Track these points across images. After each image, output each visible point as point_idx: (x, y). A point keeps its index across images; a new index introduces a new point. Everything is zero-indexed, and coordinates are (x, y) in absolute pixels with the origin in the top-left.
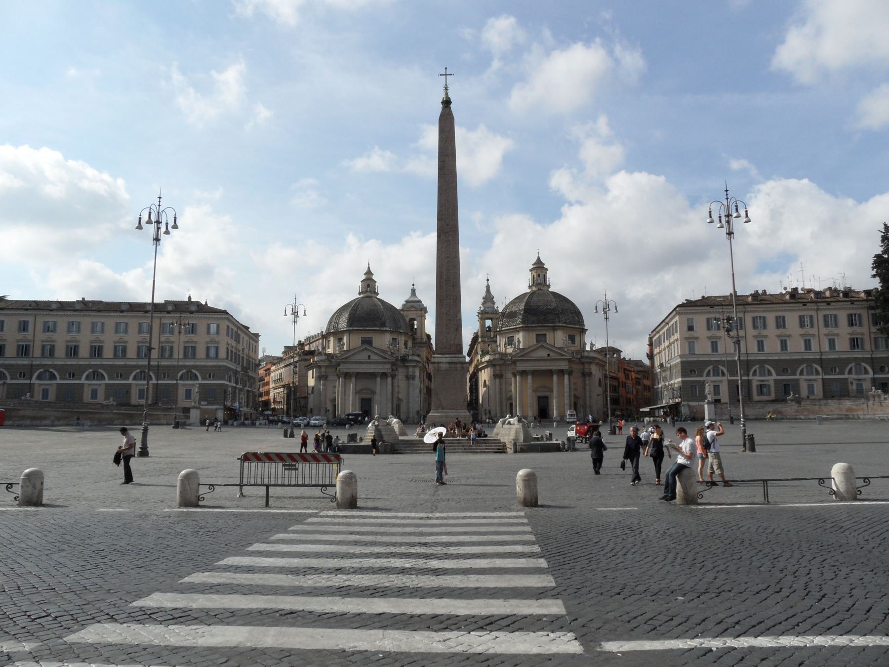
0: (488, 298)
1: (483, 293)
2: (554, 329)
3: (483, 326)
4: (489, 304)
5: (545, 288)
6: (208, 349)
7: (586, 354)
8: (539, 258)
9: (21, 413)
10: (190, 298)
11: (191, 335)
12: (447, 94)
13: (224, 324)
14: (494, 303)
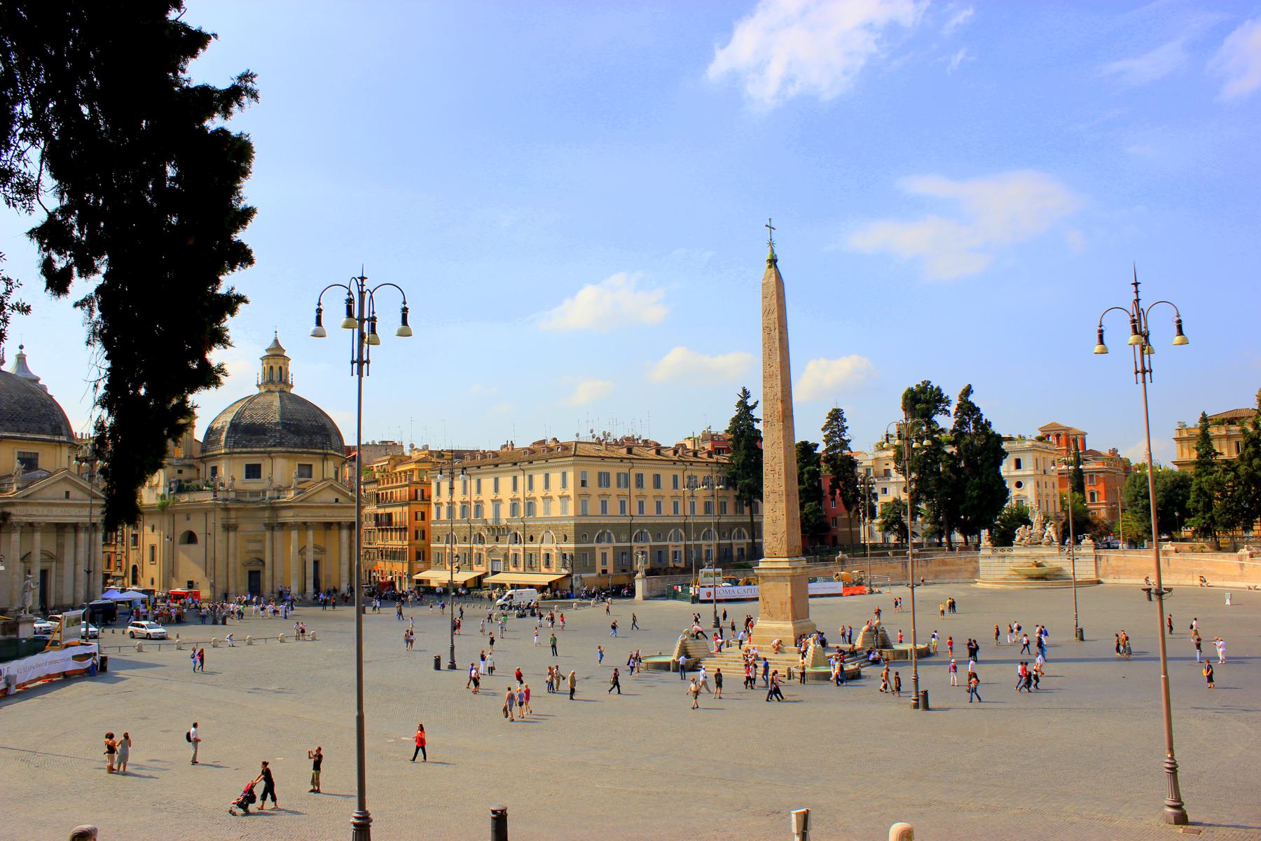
2: (325, 457)
8: (276, 341)
12: (772, 251)
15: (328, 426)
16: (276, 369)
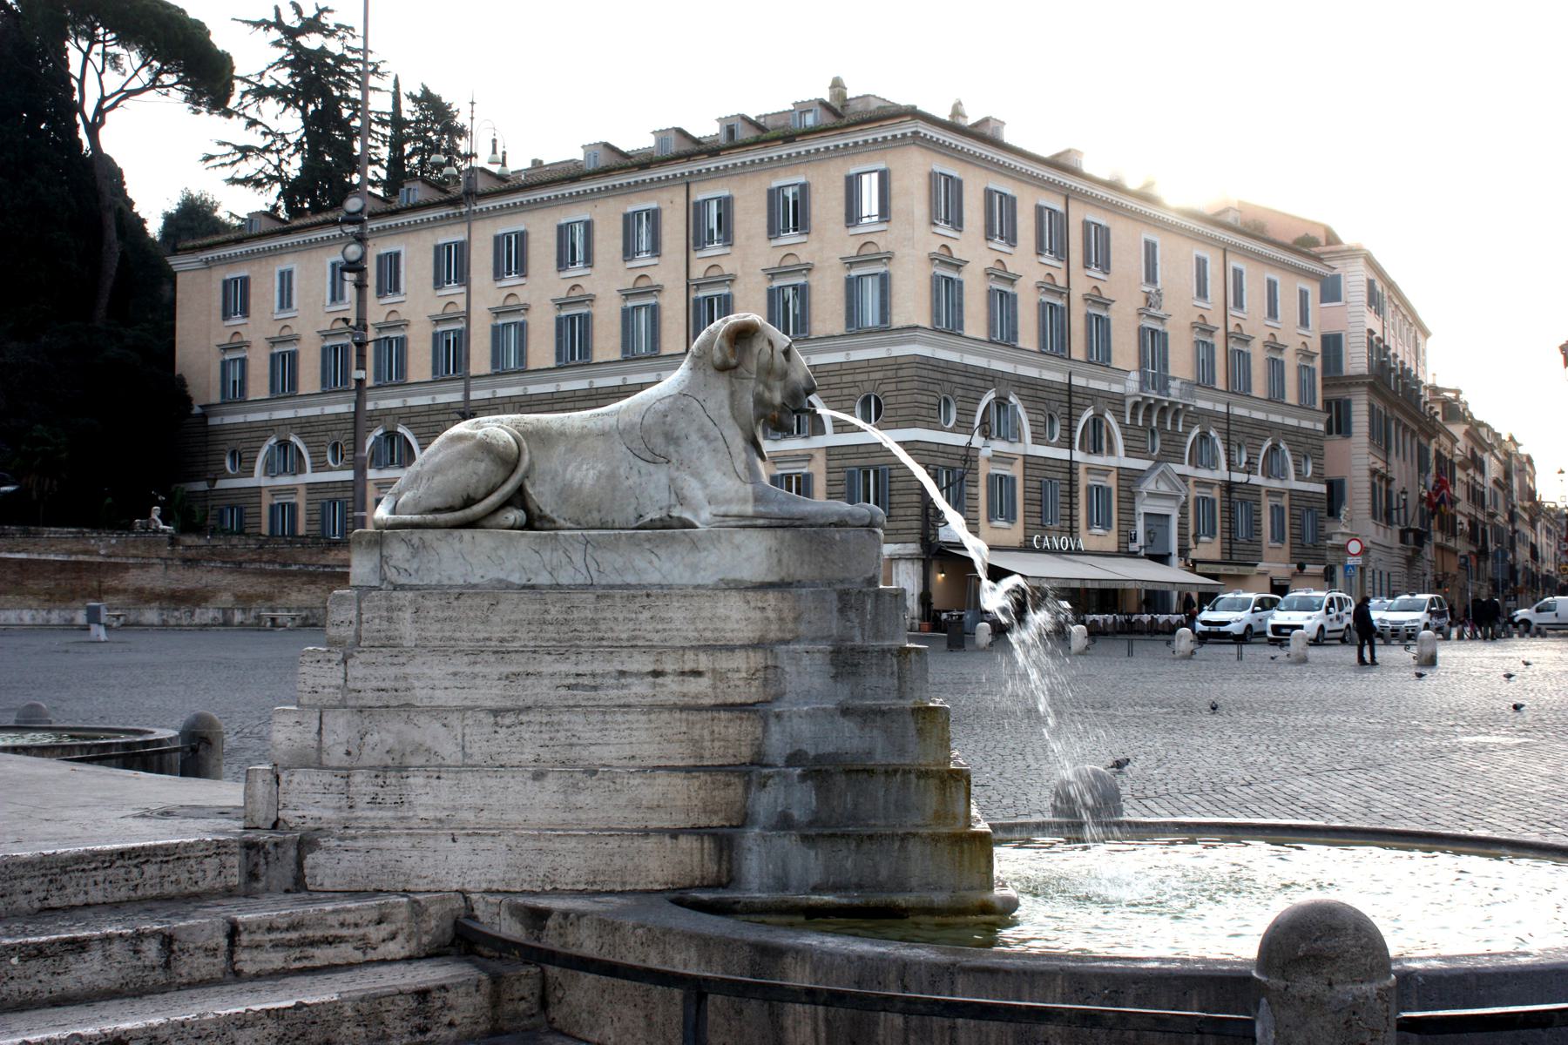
6: (852, 287)
9: (134, 579)
10: (837, 85)
11: (791, 238)
13: (913, 171)
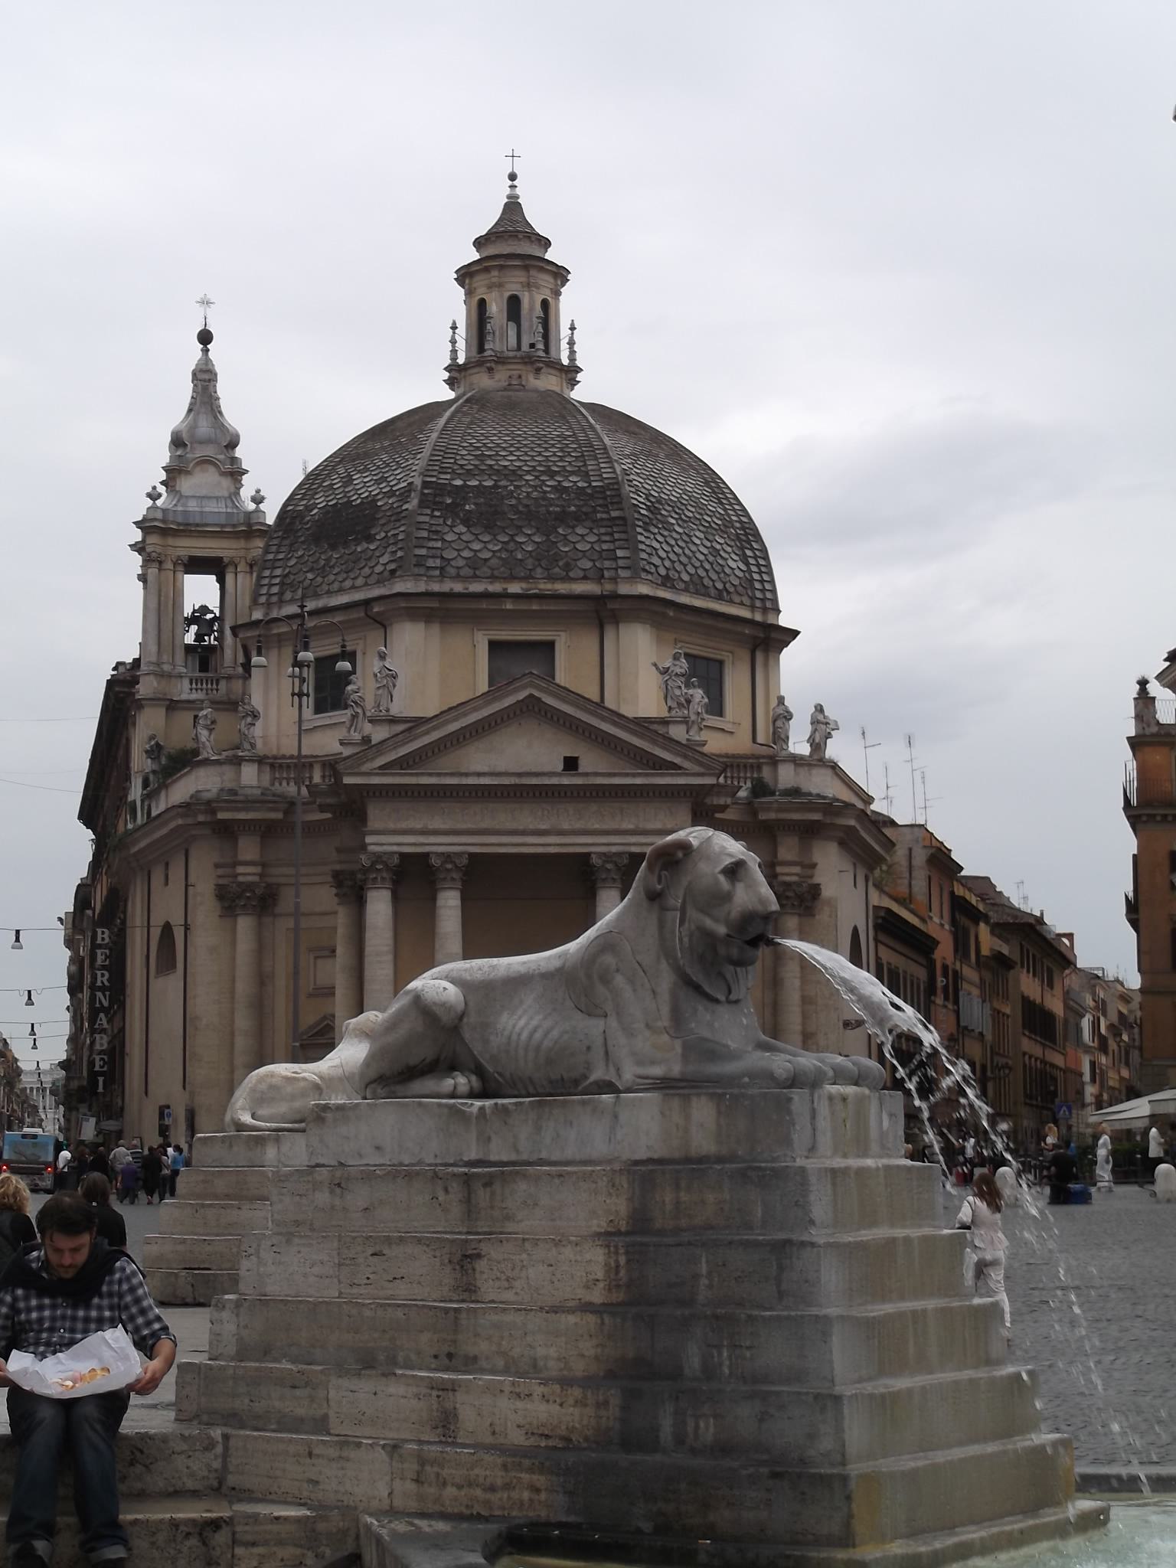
0: (204, 444)
1: (173, 408)
2: (604, 613)
3: (162, 605)
4: (200, 482)
5: (549, 382)
7: (786, 777)
8: (513, 207)
14: (236, 473)
15: (643, 484)
16: (496, 308)
